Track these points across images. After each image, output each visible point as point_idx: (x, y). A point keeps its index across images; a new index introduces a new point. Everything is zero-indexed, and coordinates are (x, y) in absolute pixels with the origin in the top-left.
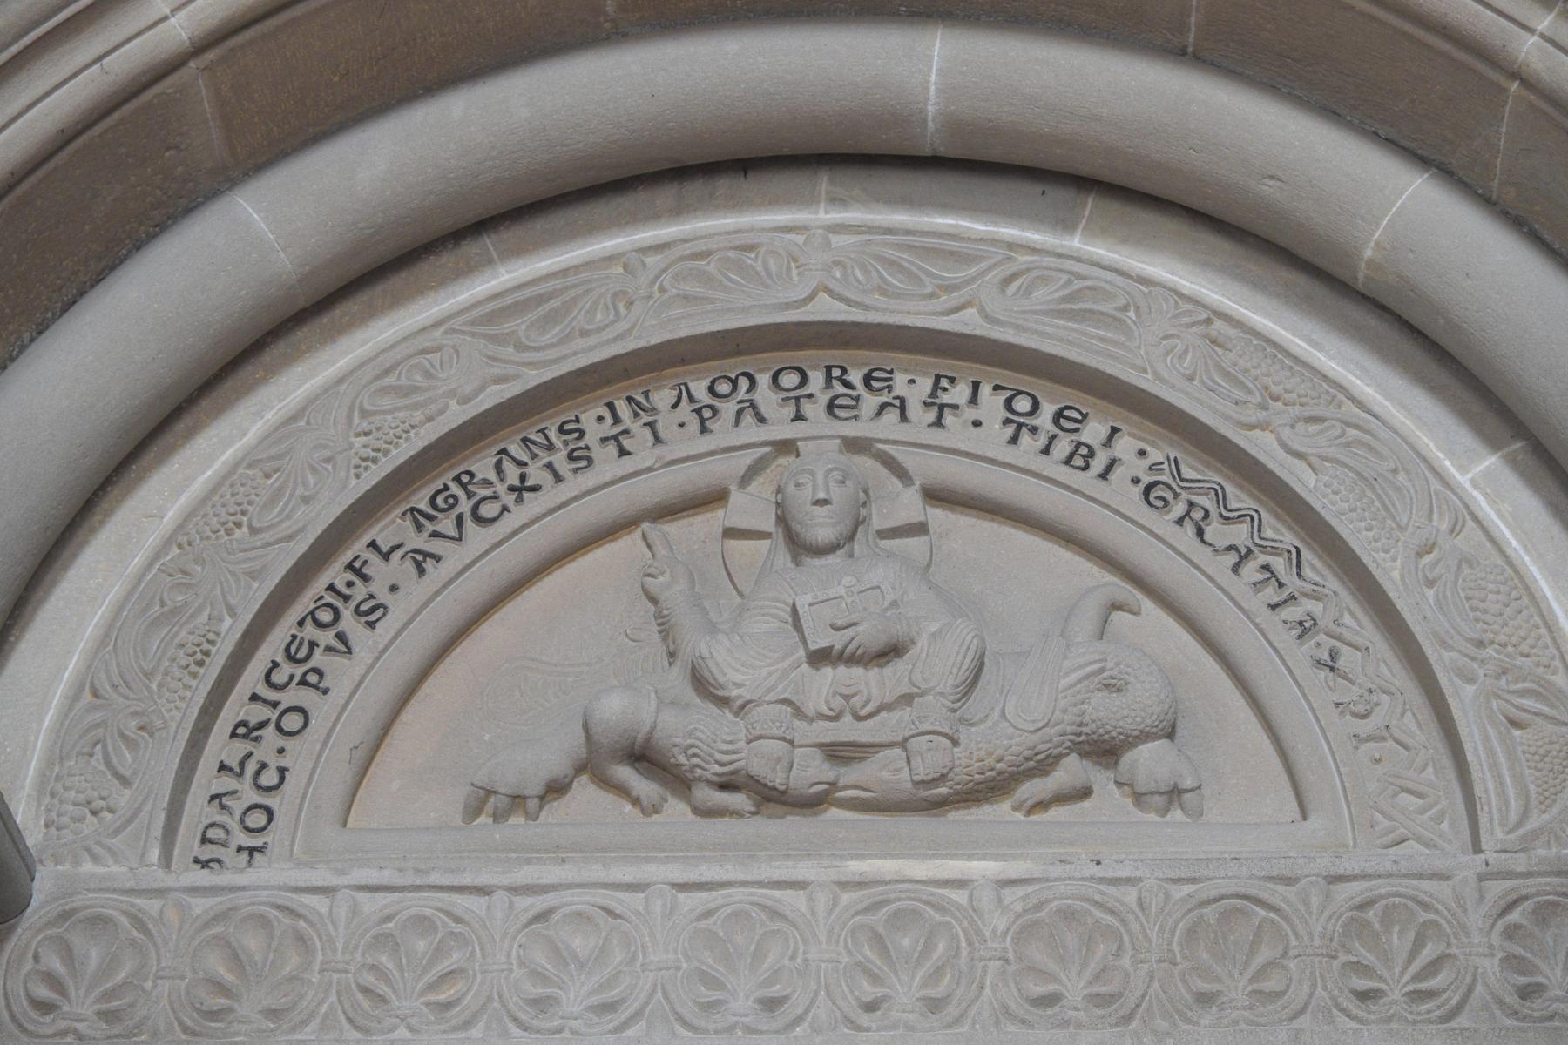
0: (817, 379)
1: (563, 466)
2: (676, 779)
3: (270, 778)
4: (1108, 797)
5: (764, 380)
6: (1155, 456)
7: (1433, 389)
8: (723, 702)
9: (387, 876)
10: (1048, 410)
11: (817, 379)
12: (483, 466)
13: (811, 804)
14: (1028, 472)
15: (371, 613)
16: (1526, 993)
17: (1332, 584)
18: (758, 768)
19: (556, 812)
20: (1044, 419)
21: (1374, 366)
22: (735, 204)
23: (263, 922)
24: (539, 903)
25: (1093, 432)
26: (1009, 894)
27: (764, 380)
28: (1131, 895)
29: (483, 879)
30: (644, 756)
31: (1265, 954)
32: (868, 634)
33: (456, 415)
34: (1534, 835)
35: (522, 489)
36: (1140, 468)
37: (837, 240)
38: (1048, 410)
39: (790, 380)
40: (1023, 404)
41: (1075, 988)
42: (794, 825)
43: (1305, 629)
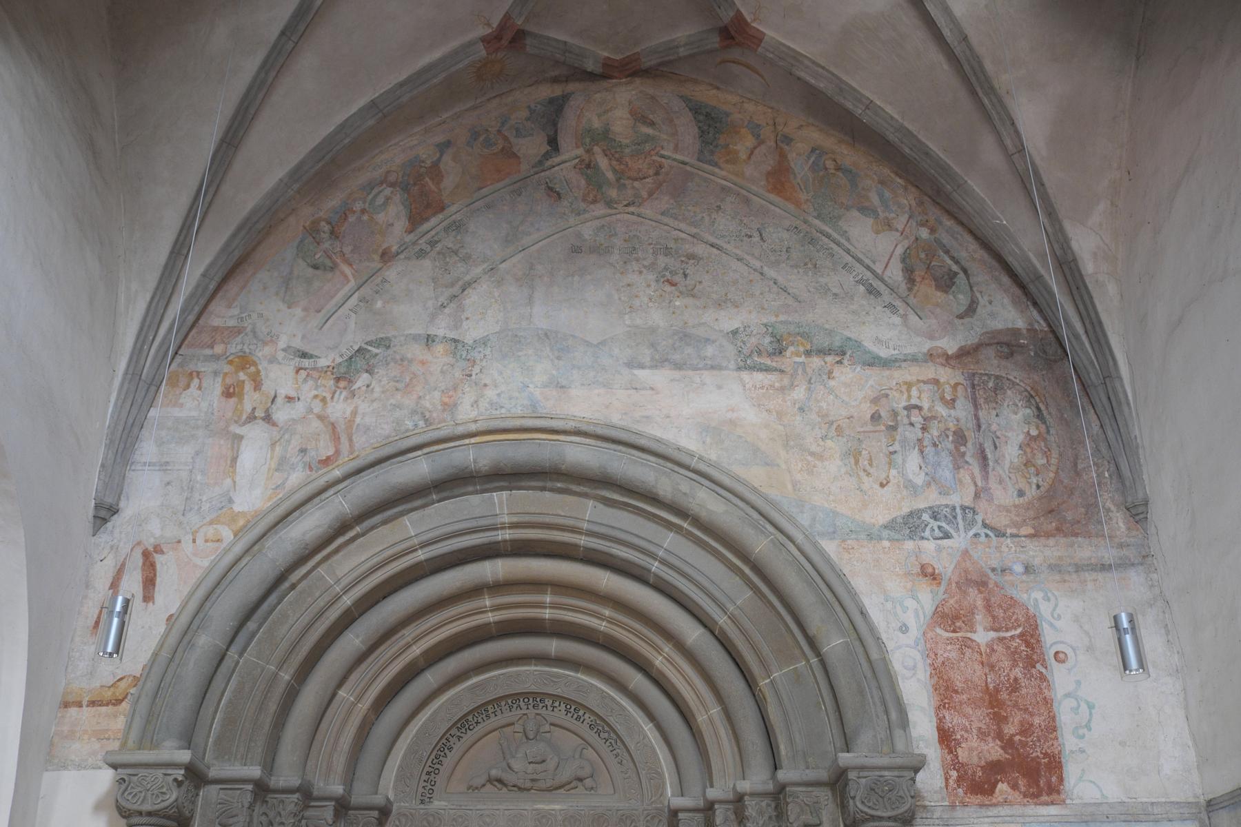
2: (506, 785)
4: (581, 789)
12: (470, 718)
14: (569, 721)
15: (450, 749)
19: (483, 790)
25: (581, 713)
30: (500, 781)
32: (539, 759)
33: (466, 710)
43: (617, 756)
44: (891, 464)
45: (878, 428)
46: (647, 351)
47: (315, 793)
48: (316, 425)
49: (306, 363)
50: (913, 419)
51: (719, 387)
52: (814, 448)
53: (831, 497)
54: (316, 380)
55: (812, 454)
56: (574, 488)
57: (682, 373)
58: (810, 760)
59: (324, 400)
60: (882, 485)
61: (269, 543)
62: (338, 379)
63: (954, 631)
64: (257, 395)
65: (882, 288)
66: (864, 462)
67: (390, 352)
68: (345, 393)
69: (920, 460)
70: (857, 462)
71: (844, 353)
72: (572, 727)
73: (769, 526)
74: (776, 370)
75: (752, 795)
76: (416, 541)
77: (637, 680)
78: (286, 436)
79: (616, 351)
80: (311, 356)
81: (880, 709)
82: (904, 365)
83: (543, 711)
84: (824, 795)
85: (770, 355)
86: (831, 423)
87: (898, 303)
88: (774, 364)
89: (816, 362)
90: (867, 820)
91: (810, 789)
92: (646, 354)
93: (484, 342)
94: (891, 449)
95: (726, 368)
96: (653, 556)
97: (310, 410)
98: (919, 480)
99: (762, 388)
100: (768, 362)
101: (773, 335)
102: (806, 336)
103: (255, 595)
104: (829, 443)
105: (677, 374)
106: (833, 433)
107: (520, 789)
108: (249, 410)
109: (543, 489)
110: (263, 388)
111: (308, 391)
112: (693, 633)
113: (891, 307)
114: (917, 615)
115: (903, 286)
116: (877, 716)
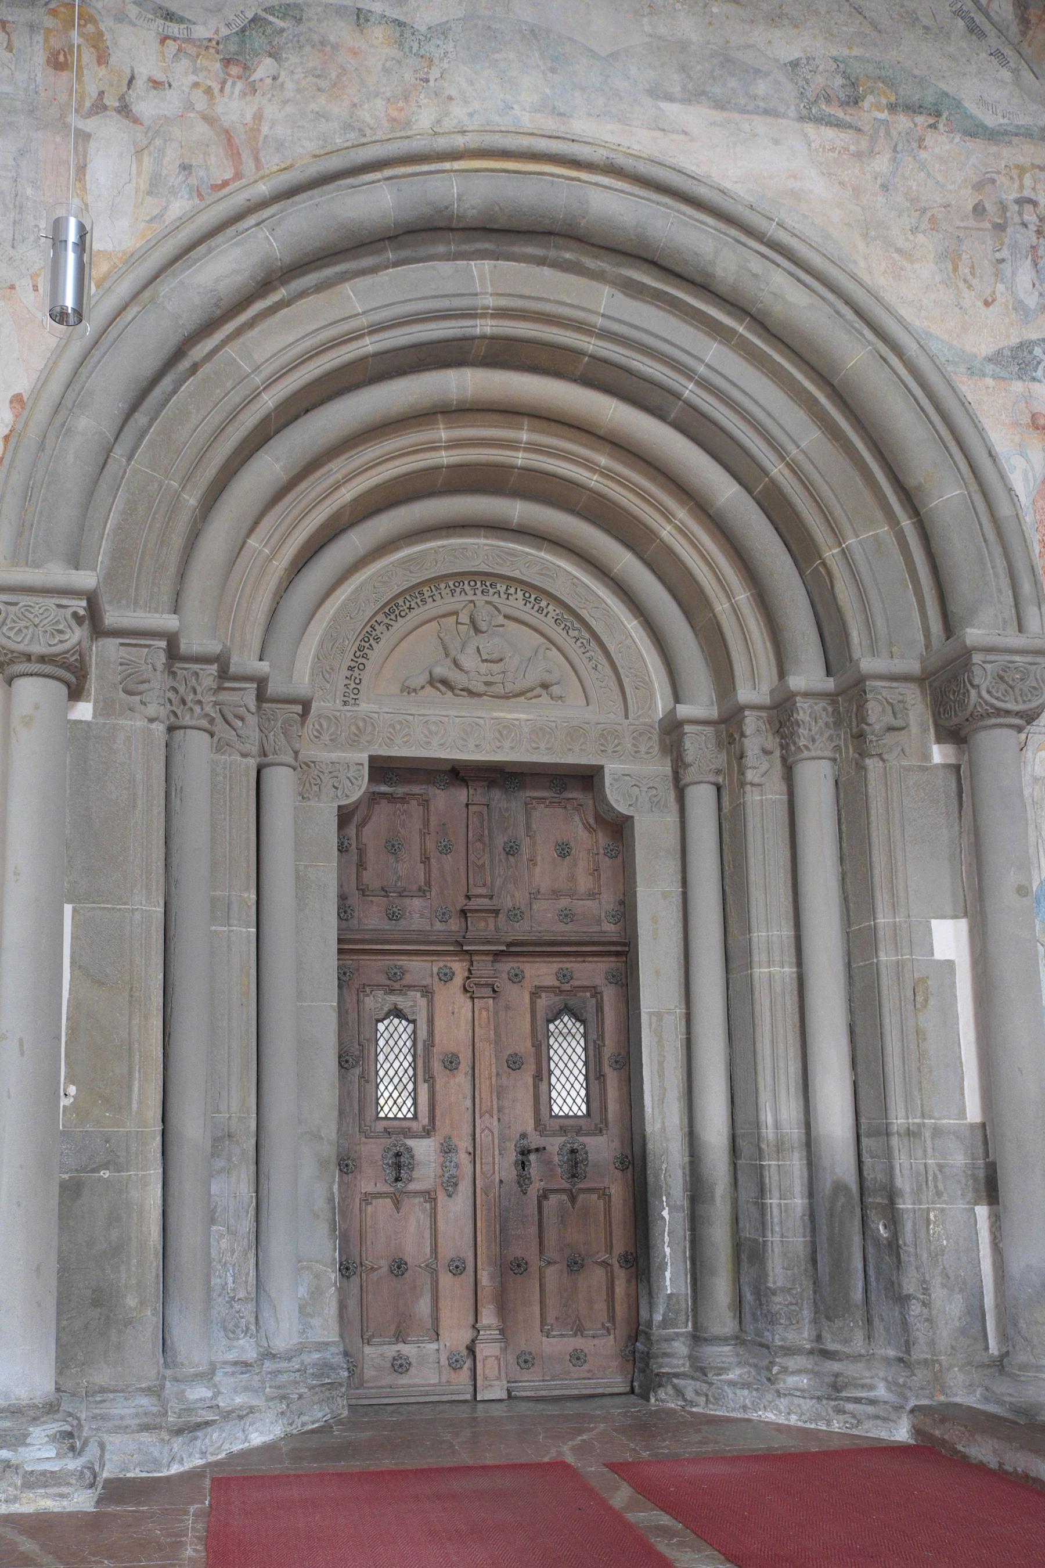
0: (479, 584)
1: (420, 603)
3: (357, 681)
5: (466, 583)
6: (558, 611)
7: (623, 602)
8: (463, 670)
9: (391, 710)
10: (533, 597)
11: (479, 584)
12: (400, 601)
13: (479, 695)
15: (377, 639)
16: (636, 752)
17: (597, 648)
18: (471, 687)
19: (421, 693)
20: (532, 599)
21: (612, 596)
22: (462, 536)
23: (364, 720)
24: (426, 719)
25: (543, 604)
26: (528, 723)
27: (466, 583)
28: (554, 724)
29: (413, 712)
30: (444, 682)
31: (582, 740)
33: (397, 590)
34: (639, 716)
35: (410, 608)
36: (553, 614)
37: (486, 548)
38: (533, 597)
39: (472, 583)
40: (527, 595)
41: (543, 746)
42: (475, 700)
43: (590, 659)
44: (998, 275)
45: (982, 225)
46: (676, 77)
47: (232, 670)
48: (201, 129)
49: (174, 29)
50: (1026, 218)
51: (777, 142)
52: (901, 243)
53: (923, 313)
54: (194, 59)
55: (899, 251)
56: (589, 263)
57: (725, 114)
58: (895, 649)
59: (209, 91)
60: (987, 304)
61: (165, 288)
62: (227, 62)
64: (102, 72)
65: (987, 27)
66: (964, 270)
67: (303, 28)
68: (240, 86)
69: (1034, 274)
70: (955, 270)
71: (939, 115)
72: (534, 622)
73: (867, 332)
74: (850, 127)
75: (807, 695)
76: (364, 321)
77: (624, 561)
78: (158, 142)
79: (633, 71)
80: (181, 20)
82: (1016, 140)
83: (495, 599)
84: (912, 694)
85: (842, 104)
86: (924, 211)
87: (1008, 51)
88: (848, 118)
89: (903, 121)
91: (894, 684)
92: (675, 82)
93: (443, 30)
94: (998, 255)
95: (784, 116)
96: (687, 373)
97: (189, 106)
98: (1032, 301)
99: (833, 150)
100: (840, 113)
101: (846, 76)
102: (890, 83)
103: (150, 365)
104: (921, 238)
105: (718, 116)
106: (925, 225)
107: (471, 693)
108: (95, 94)
109: (541, 261)
110: (113, 60)
111: (183, 75)
112: (724, 490)
113: (997, 54)
114: (1026, 479)
115: (1014, 28)
116: (1000, 591)
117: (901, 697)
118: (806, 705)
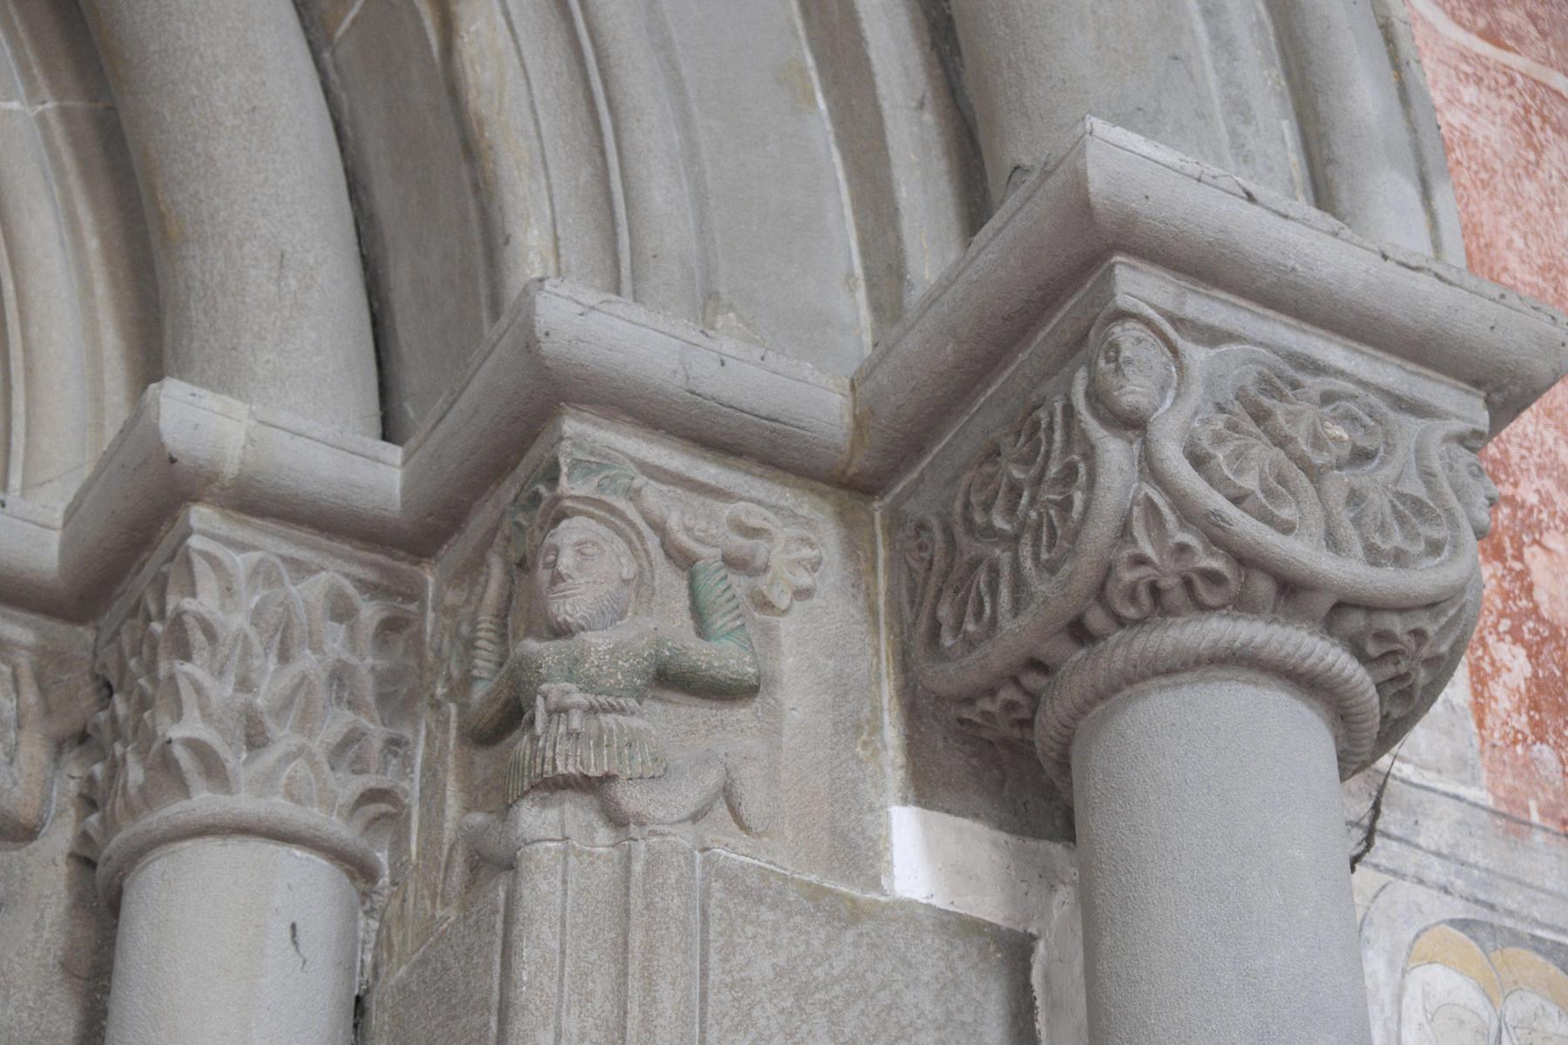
63: (1491, 36)
75: (257, 502)
81: (1262, 80)
90: (1198, 593)
91: (709, 471)
117: (738, 542)
118: (240, 562)
